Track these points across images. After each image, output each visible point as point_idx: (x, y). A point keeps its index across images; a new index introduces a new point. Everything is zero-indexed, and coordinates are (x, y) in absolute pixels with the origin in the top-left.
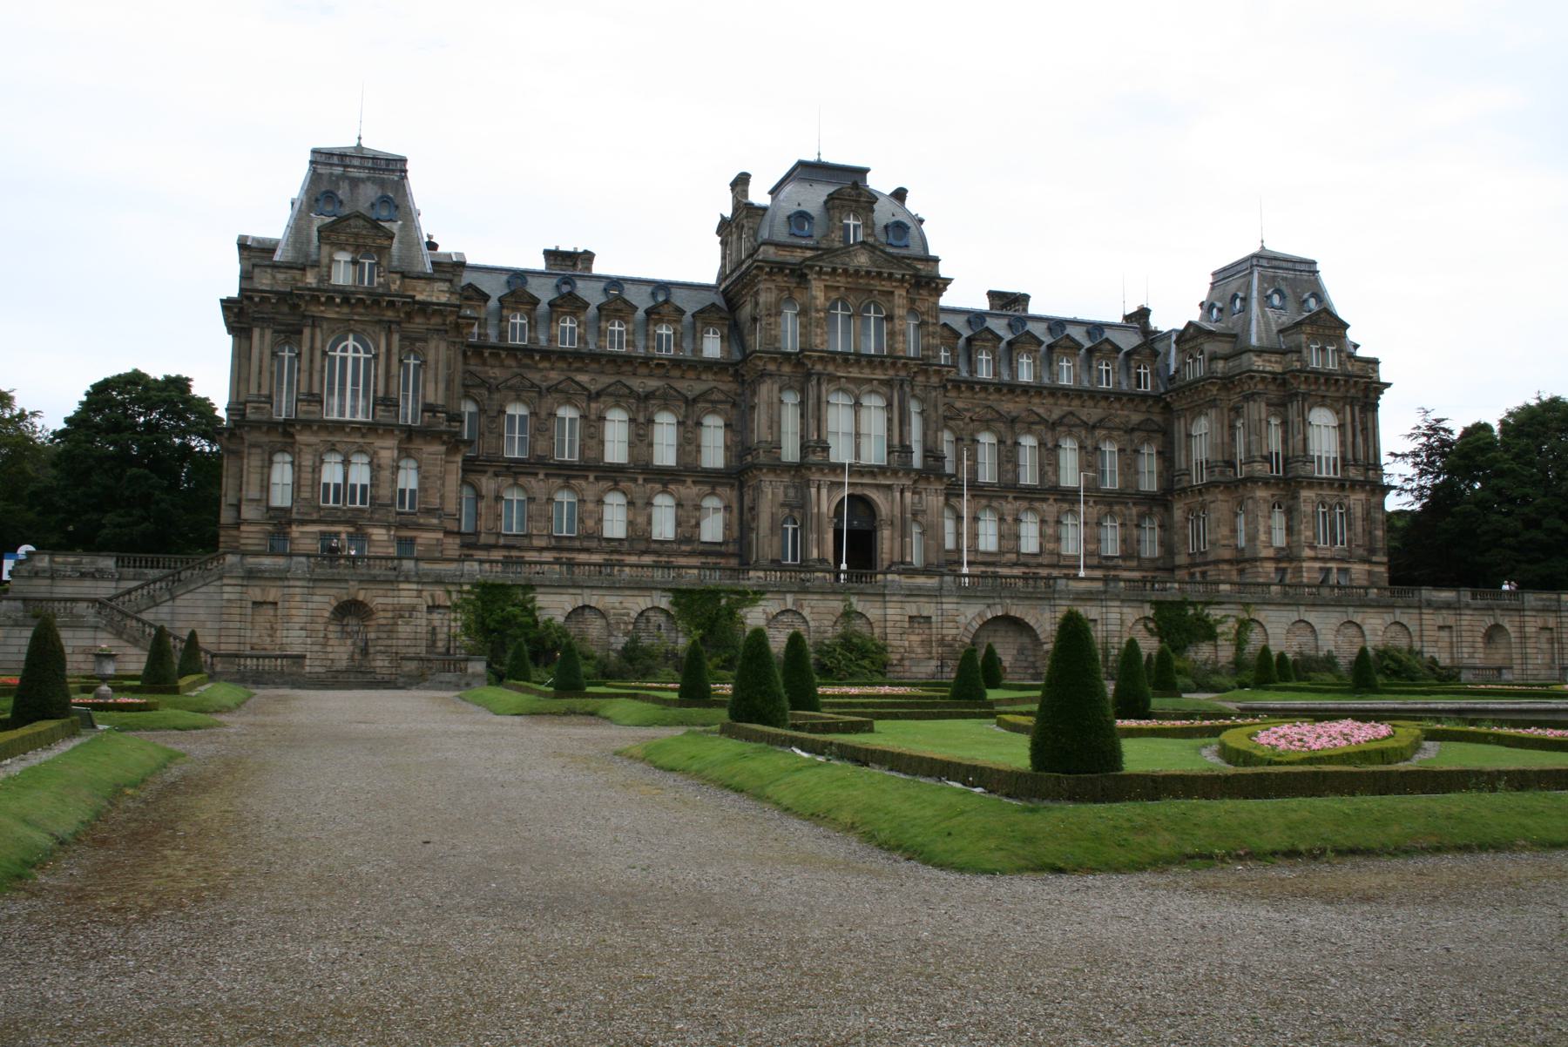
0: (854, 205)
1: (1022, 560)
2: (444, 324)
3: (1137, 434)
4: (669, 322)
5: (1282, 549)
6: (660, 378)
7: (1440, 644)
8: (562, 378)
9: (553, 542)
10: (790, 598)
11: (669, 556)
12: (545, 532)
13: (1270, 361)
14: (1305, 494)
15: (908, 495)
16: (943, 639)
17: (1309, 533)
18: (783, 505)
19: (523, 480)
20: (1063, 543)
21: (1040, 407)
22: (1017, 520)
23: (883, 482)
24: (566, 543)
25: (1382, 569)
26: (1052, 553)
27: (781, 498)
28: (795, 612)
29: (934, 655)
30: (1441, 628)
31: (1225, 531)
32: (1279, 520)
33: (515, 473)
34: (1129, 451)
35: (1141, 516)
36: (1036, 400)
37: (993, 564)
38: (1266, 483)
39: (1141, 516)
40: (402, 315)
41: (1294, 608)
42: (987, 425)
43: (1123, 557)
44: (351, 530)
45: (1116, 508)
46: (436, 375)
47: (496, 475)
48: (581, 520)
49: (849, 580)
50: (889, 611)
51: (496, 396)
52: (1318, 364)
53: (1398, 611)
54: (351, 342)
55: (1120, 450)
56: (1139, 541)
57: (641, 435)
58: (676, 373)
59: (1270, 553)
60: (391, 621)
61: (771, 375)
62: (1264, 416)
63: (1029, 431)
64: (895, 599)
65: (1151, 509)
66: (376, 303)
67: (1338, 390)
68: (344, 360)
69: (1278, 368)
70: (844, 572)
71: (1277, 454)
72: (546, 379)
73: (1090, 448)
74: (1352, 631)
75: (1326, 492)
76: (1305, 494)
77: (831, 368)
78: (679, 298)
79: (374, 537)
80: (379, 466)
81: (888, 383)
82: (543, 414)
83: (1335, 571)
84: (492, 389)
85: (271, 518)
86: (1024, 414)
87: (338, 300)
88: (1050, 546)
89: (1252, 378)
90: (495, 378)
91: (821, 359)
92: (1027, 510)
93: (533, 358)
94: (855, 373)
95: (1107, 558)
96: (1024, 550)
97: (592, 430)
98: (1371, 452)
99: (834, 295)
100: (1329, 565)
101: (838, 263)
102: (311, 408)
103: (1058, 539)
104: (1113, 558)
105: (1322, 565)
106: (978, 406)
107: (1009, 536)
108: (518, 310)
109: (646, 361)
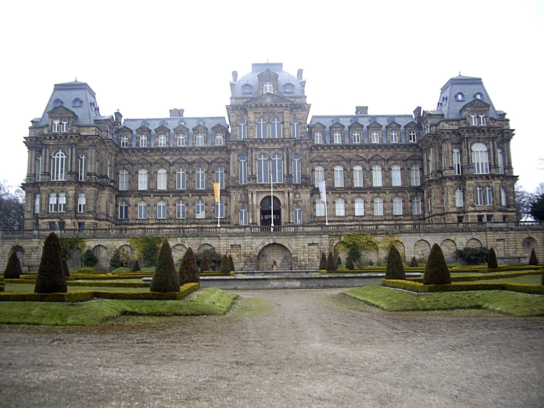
0: (268, 78)
1: (356, 219)
2: (94, 143)
3: (408, 162)
4: (201, 133)
5: (461, 208)
6: (197, 155)
7: (498, 248)
8: (159, 158)
9: (157, 221)
10: (179, 239)
11: (202, 224)
12: (154, 218)
13: (453, 125)
14: (468, 182)
15: (291, 194)
16: (245, 254)
17: (472, 200)
18: (239, 202)
19: (145, 198)
20: (375, 210)
21: (362, 153)
22: (353, 202)
23: (280, 190)
24: (162, 221)
26: (369, 215)
27: (239, 199)
28: (182, 245)
29: (242, 260)
30: (498, 240)
31: (438, 201)
32: (459, 195)
33: (142, 196)
34: (405, 169)
35: (412, 197)
36: (360, 151)
37: (342, 221)
38: (451, 178)
39: (412, 197)
40: (76, 141)
41: (418, 234)
42: (338, 163)
43: (404, 215)
44: (59, 220)
45: (400, 194)
46: (91, 162)
47: (135, 197)
48: (168, 212)
49: (274, 230)
50: (221, 243)
51: (135, 167)
52: (475, 124)
53: (474, 233)
54: (60, 152)
55: (401, 169)
56: (411, 208)
57: (152, 178)
58: (203, 153)
59: (455, 210)
60: (30, 253)
61: (234, 150)
62: (450, 149)
63: (358, 164)
64: (223, 238)
65: (416, 194)
66: (66, 137)
67: (485, 135)
68: (58, 159)
69: (456, 127)
70: (273, 227)
71: (458, 165)
72: (153, 159)
73: (386, 169)
74: (451, 243)
75: (480, 181)
76: (468, 182)
77: (256, 146)
78: (322, 121)
79: (67, 223)
80: (68, 197)
81: (282, 149)
82: (152, 173)
83: (485, 216)
84: (171, 165)
85: (35, 217)
86: (355, 157)
87: (53, 138)
88: (369, 212)
89: (443, 133)
90: (134, 161)
91: (251, 142)
92: (357, 197)
93: (147, 151)
94: (267, 146)
95: (396, 216)
96: (337, 214)
97: (171, 177)
98: (507, 161)
99: (259, 116)
100: (482, 214)
101: (258, 103)
102: (45, 177)
103: (373, 209)
104: (399, 216)
105: (478, 214)
106: (334, 155)
108: (143, 134)
109: (191, 149)
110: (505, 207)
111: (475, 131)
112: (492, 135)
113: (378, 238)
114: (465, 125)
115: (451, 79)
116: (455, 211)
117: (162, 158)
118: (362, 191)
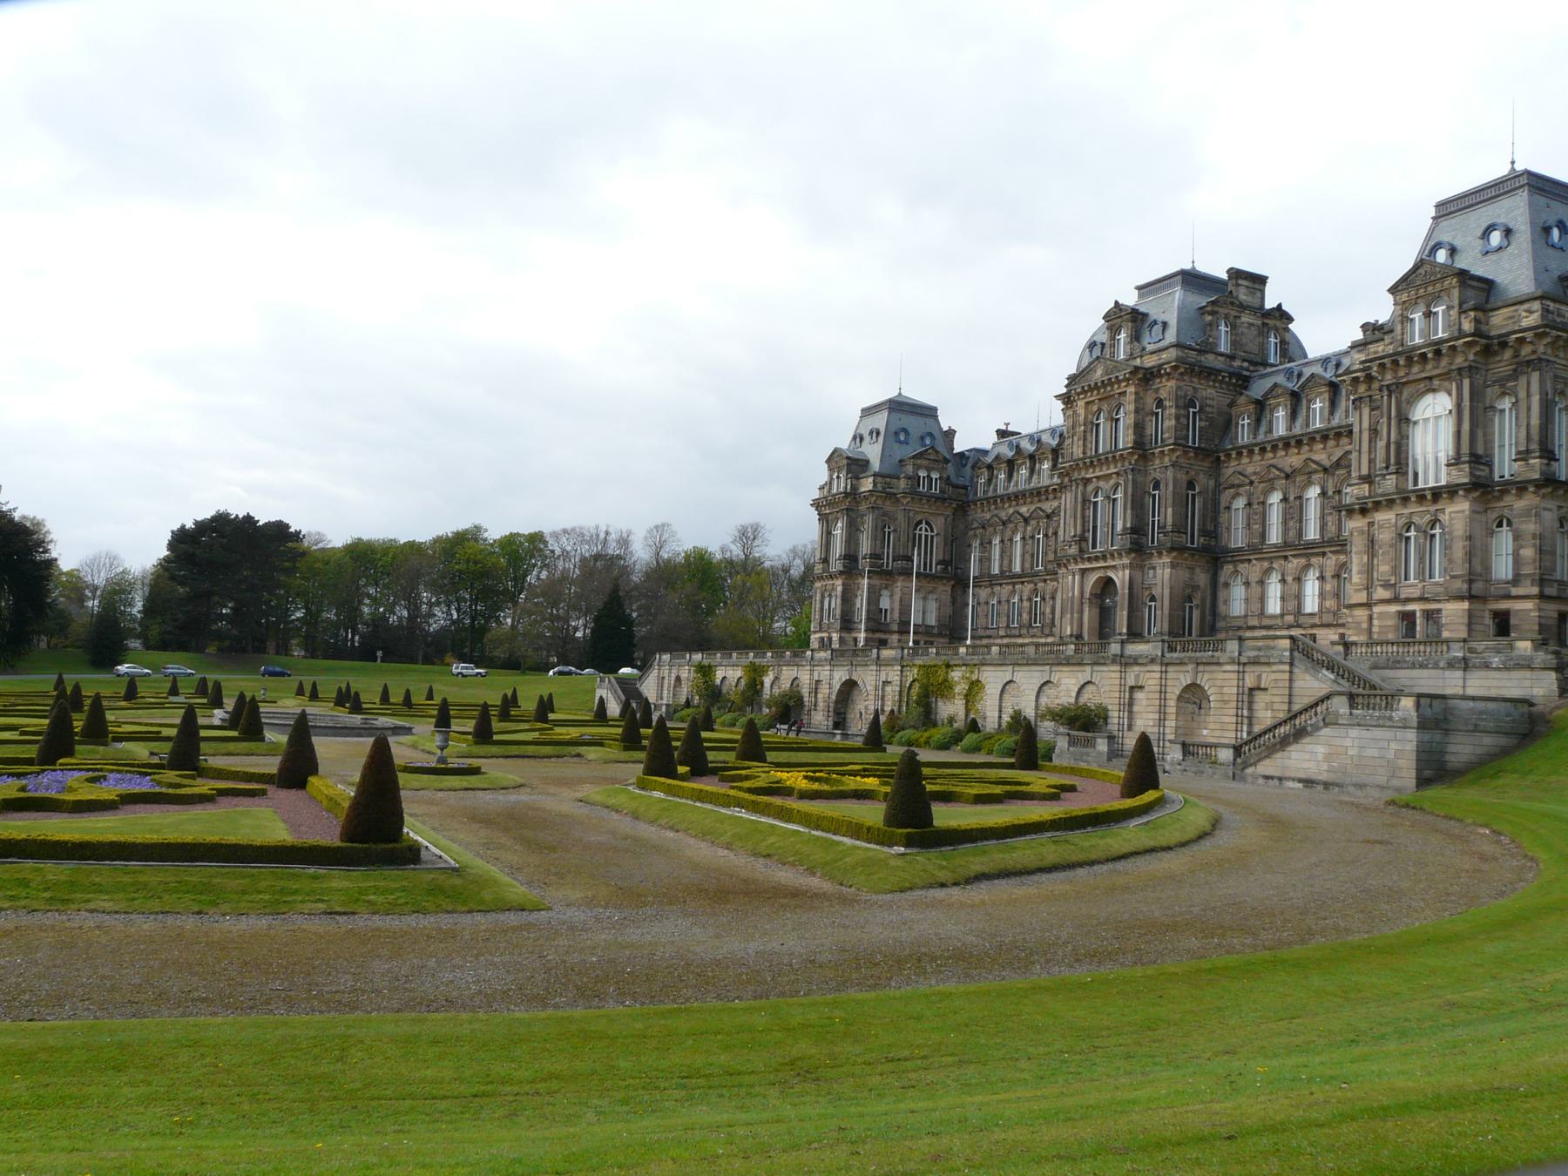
14: (1384, 517)
21: (1321, 455)
24: (1014, 632)
25: (1529, 605)
53: (1088, 669)
62: (1366, 424)
63: (1309, 483)
75: (1413, 508)
77: (1083, 474)
107: (1293, 598)
110: (1507, 583)
111: (1402, 362)
112: (1459, 360)
114: (1391, 347)
115: (1439, 205)
116: (1365, 601)
117: (1018, 512)
118: (1316, 550)
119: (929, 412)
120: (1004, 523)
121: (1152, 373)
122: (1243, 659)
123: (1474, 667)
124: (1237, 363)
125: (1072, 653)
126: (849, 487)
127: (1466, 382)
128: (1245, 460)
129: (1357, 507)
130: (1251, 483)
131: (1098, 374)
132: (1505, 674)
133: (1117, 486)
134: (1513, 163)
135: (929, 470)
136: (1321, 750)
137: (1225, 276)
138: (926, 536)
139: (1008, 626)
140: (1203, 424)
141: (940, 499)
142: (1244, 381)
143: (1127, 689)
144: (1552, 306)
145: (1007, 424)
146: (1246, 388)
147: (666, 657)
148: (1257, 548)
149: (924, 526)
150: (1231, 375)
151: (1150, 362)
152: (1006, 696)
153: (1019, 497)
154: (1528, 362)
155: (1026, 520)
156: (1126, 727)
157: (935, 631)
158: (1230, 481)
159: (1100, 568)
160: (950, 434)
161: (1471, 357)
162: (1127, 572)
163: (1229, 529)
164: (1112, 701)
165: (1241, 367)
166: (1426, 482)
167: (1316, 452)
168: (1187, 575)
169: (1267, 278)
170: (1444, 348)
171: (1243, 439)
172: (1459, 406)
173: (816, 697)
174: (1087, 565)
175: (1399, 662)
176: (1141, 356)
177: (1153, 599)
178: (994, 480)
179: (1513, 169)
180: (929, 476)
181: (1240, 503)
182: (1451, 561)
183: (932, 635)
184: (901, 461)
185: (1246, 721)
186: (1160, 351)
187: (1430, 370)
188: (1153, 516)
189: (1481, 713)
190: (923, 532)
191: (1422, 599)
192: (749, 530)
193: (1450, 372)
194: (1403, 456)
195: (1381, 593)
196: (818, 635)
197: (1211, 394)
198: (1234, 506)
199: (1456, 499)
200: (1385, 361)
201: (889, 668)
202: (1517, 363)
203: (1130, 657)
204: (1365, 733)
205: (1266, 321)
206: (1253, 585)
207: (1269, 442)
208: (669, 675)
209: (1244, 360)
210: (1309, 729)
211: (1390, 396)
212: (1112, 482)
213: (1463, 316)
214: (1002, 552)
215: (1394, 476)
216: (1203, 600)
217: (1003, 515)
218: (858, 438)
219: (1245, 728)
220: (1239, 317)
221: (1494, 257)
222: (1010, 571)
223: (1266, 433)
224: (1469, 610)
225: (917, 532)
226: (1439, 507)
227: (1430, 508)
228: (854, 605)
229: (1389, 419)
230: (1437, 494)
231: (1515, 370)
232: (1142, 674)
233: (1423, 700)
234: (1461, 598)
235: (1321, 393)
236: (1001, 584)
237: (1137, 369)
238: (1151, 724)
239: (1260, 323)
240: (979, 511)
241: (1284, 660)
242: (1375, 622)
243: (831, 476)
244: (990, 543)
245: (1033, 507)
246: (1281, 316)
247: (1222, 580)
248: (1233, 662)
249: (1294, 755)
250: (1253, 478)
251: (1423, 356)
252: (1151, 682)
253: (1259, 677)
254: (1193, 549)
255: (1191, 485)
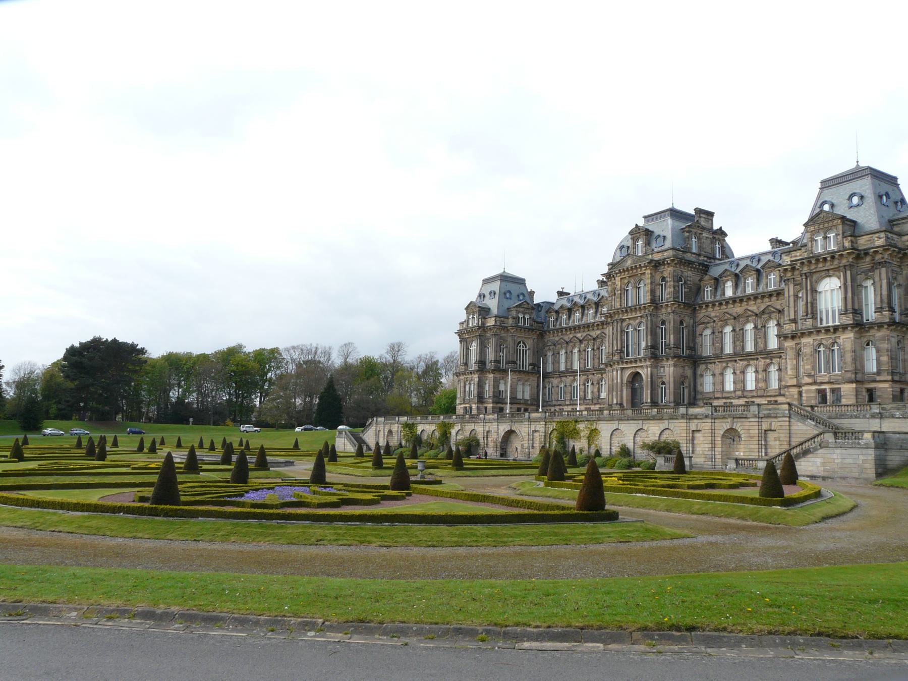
14: (805, 340)
17: (808, 367)
21: (753, 307)
25: (886, 385)
53: (666, 422)
62: (792, 293)
63: (748, 322)
75: (822, 336)
77: (621, 316)
88: (760, 385)
105: (817, 387)
107: (740, 382)
110: (874, 374)
111: (813, 261)
112: (844, 261)
113: (581, 425)
114: (806, 254)
116: (796, 384)
117: (575, 337)
118: (753, 357)
119: (521, 282)
120: (567, 343)
121: (659, 263)
122: (761, 415)
123: (886, 417)
124: (701, 258)
125: (655, 413)
126: (480, 323)
127: (848, 273)
128: (710, 309)
129: (790, 335)
130: (714, 321)
131: (629, 263)
132: (903, 421)
133: (640, 323)
134: (858, 162)
135: (524, 313)
136: (819, 460)
137: (693, 213)
138: (523, 350)
139: (571, 399)
140: (686, 290)
141: (530, 330)
142: (706, 268)
143: (691, 431)
144: (890, 235)
145: (563, 288)
146: (707, 271)
147: (381, 419)
148: (719, 356)
149: (522, 344)
150: (700, 264)
151: (657, 257)
152: (614, 437)
153: (576, 328)
154: (879, 263)
155: (581, 341)
156: (691, 452)
157: (529, 402)
158: (702, 321)
159: (632, 367)
160: (532, 293)
161: (851, 260)
162: (649, 369)
163: (702, 346)
164: (681, 438)
165: (704, 260)
166: (827, 322)
167: (751, 305)
168: (681, 371)
169: (714, 213)
170: (837, 256)
171: (708, 298)
172: (845, 284)
173: (487, 440)
174: (625, 366)
175: (843, 415)
176: (652, 254)
177: (663, 383)
178: (559, 319)
179: (858, 165)
180: (524, 317)
181: (708, 332)
182: (845, 363)
183: (528, 405)
184: (508, 309)
185: (763, 447)
186: (663, 251)
187: (828, 265)
188: (662, 339)
189: (903, 440)
190: (522, 348)
191: (829, 383)
192: (396, 346)
193: (839, 267)
194: (814, 309)
195: (807, 380)
196: (462, 406)
197: (690, 275)
198: (704, 334)
199: (846, 332)
200: (804, 261)
201: (538, 423)
202: (874, 263)
203: (692, 415)
204: (844, 451)
205: (715, 236)
206: (717, 375)
207: (724, 300)
208: (384, 430)
209: (705, 257)
210: (811, 450)
211: (806, 279)
212: (638, 321)
213: (845, 239)
214: (567, 359)
215: (811, 320)
216: (690, 385)
217: (566, 338)
218: (482, 296)
219: (763, 450)
220: (702, 234)
221: (855, 209)
222: (572, 369)
223: (721, 295)
224: (856, 388)
225: (518, 348)
226: (837, 335)
227: (832, 336)
228: (484, 389)
229: (807, 290)
230: (836, 329)
231: (873, 267)
232: (699, 424)
233: (875, 434)
234: (852, 382)
235: (752, 275)
236: (566, 376)
237: (652, 261)
238: (707, 450)
239: (711, 237)
240: (551, 336)
241: (786, 415)
242: (804, 395)
243: (468, 317)
244: (559, 353)
245: (585, 334)
246: (721, 233)
247: (699, 373)
248: (755, 416)
249: (803, 463)
250: (715, 319)
251: (825, 259)
252: (706, 428)
253: (771, 424)
254: (684, 357)
255: (681, 323)
